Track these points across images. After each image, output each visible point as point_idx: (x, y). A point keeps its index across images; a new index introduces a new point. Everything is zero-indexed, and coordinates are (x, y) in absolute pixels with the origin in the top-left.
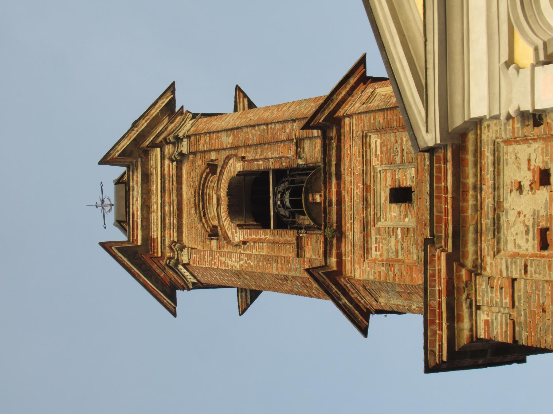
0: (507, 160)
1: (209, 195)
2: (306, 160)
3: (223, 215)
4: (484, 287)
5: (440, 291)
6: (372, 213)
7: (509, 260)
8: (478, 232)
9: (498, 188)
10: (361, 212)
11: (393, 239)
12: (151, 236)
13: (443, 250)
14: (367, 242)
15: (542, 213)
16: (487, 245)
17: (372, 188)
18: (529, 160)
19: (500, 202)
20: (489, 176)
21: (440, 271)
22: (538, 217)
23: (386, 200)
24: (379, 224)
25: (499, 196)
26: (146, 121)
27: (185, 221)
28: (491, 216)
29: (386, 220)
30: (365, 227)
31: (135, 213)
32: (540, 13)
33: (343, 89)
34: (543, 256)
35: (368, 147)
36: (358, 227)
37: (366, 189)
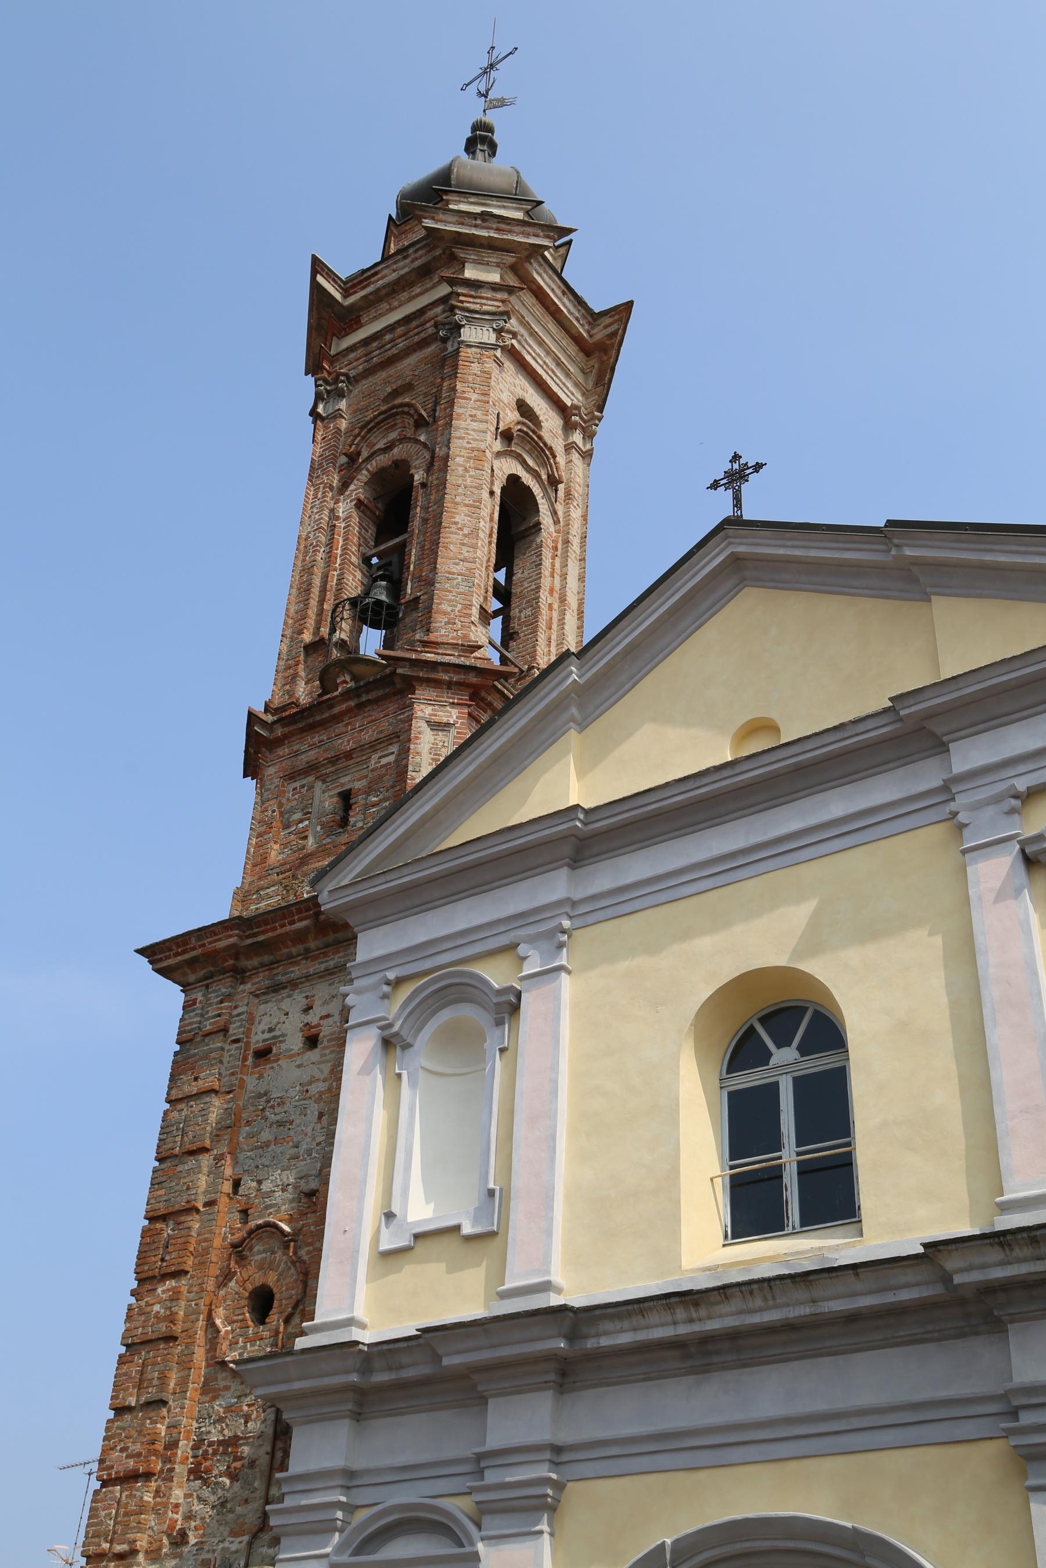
0: (333, 983)
1: (396, 424)
2: (403, 618)
3: (374, 462)
4: (223, 990)
5: (204, 945)
6: (328, 771)
7: (243, 1017)
8: (270, 966)
9: (308, 980)
10: (325, 757)
11: (297, 816)
12: (360, 316)
13: (240, 937)
14: (299, 775)
15: (283, 1046)
16: (261, 980)
17: (351, 762)
18: (328, 1016)
19: (298, 986)
20: (317, 966)
21: (220, 940)
22: (281, 1042)
23: (342, 785)
24: (319, 786)
25: (302, 983)
26: (498, 230)
27: (383, 374)
28: (284, 979)
29: (324, 792)
30: (312, 768)
31: (379, 276)
32: (434, 1013)
33: (454, 673)
34: (245, 1059)
35: (388, 742)
36: (312, 755)
37: (348, 755)
